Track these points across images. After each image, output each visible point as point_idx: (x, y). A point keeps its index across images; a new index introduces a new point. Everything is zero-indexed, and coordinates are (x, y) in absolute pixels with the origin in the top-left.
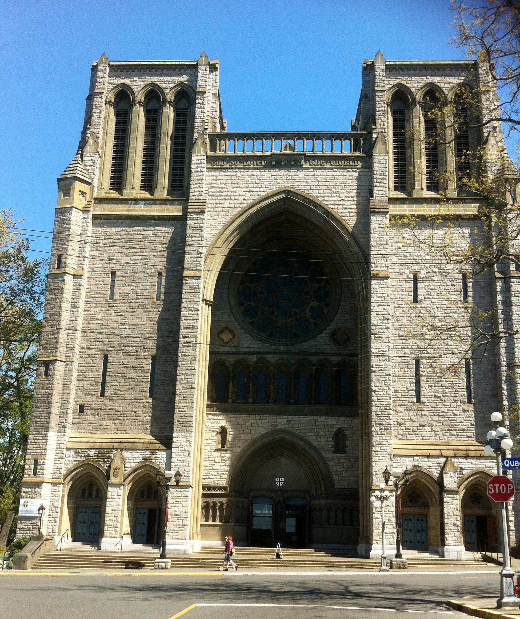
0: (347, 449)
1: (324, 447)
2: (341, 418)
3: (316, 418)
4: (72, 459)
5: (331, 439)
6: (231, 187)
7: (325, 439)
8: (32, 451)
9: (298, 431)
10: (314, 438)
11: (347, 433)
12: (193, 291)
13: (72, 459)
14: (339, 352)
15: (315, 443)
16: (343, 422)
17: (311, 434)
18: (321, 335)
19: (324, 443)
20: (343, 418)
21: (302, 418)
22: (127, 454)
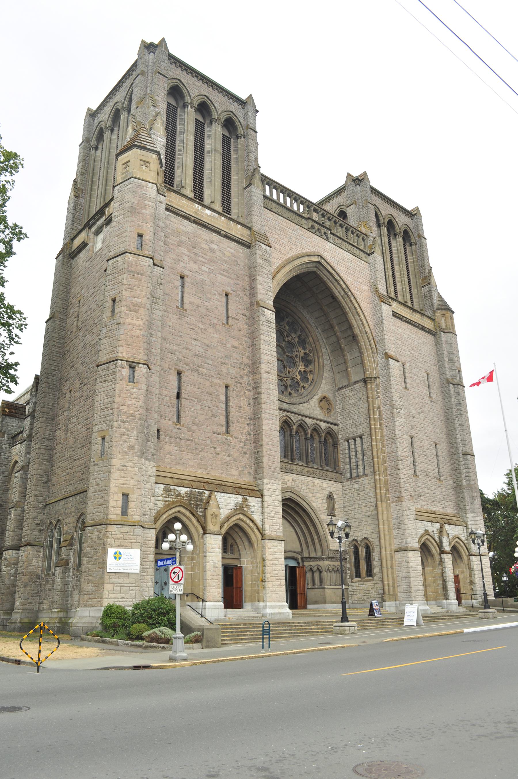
0: (336, 512)
1: (321, 509)
2: (330, 482)
3: (314, 479)
4: (161, 498)
5: (325, 501)
6: (279, 232)
7: (321, 501)
8: (118, 482)
9: (302, 491)
10: (313, 499)
11: (335, 496)
12: (269, 325)
13: (161, 498)
14: (325, 419)
15: (314, 505)
16: (331, 486)
17: (311, 495)
18: (312, 399)
19: (320, 505)
20: (332, 482)
21: (303, 478)
22: (220, 497)
